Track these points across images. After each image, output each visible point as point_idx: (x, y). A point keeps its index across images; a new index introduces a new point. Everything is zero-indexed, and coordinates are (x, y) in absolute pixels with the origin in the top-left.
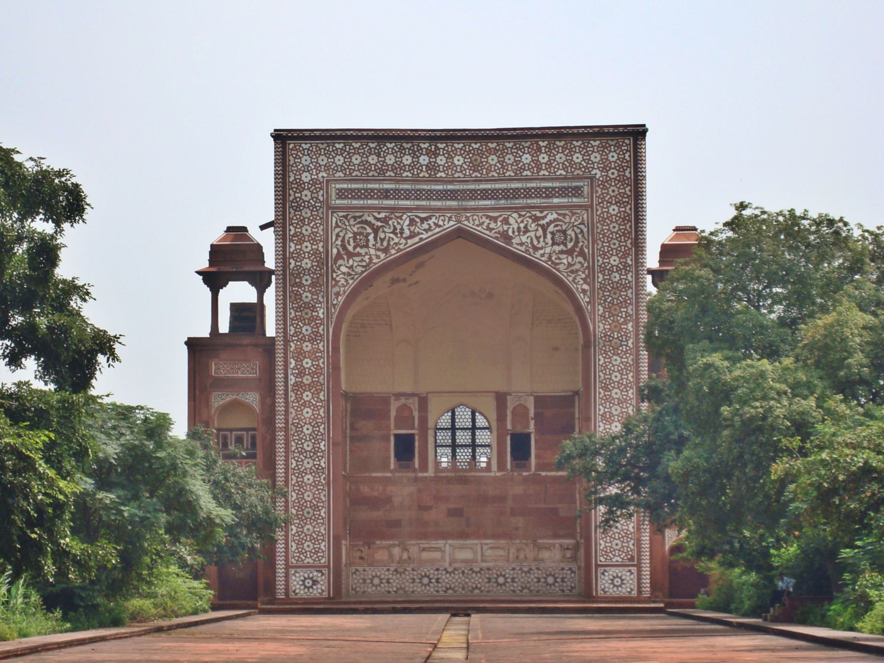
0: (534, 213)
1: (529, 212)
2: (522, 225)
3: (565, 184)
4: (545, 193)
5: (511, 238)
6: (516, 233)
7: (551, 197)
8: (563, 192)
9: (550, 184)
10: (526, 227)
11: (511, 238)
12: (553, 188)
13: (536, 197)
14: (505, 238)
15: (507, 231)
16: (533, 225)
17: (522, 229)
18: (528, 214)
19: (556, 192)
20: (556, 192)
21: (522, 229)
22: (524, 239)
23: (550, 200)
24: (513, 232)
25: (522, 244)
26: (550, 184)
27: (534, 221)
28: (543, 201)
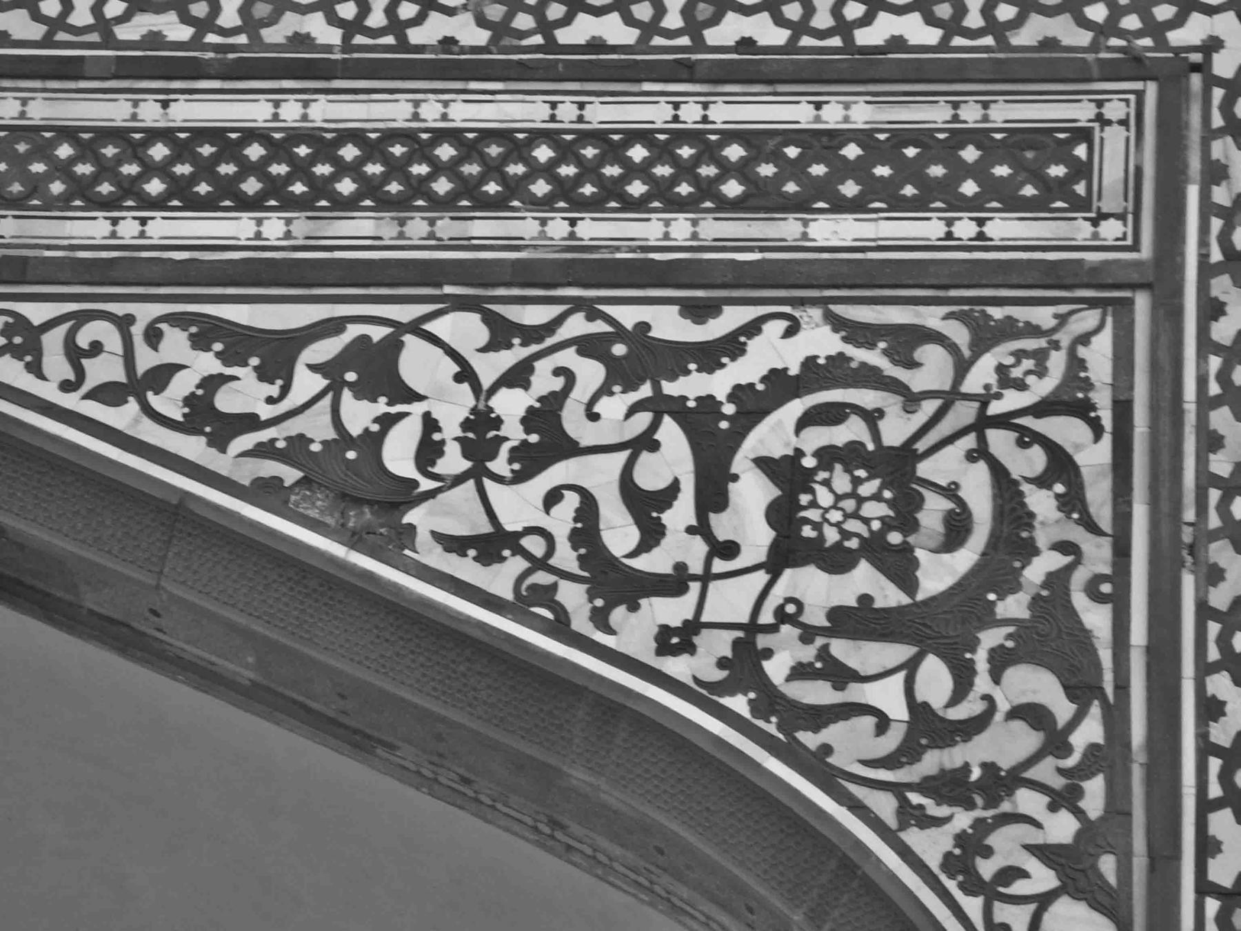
0: (628, 316)
1: (591, 310)
2: (511, 405)
3: (935, 115)
4: (742, 170)
5: (406, 494)
6: (453, 461)
7: (800, 205)
8: (902, 171)
9: (795, 113)
10: (544, 417)
11: (406, 494)
12: (823, 142)
13: (665, 198)
14: (348, 499)
15: (372, 442)
16: (614, 407)
17: (514, 432)
18: (577, 325)
19: (844, 170)
20: (858, 170)
21: (514, 432)
22: (517, 506)
23: (788, 228)
24: (428, 451)
25: (492, 544)
26: (795, 113)
27: (620, 375)
28: (713, 228)
